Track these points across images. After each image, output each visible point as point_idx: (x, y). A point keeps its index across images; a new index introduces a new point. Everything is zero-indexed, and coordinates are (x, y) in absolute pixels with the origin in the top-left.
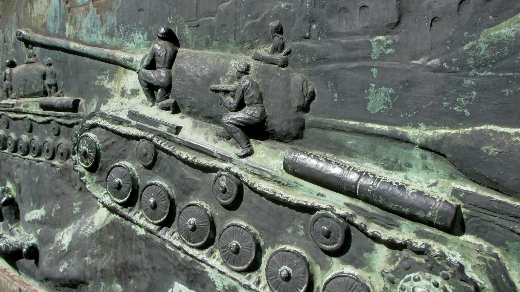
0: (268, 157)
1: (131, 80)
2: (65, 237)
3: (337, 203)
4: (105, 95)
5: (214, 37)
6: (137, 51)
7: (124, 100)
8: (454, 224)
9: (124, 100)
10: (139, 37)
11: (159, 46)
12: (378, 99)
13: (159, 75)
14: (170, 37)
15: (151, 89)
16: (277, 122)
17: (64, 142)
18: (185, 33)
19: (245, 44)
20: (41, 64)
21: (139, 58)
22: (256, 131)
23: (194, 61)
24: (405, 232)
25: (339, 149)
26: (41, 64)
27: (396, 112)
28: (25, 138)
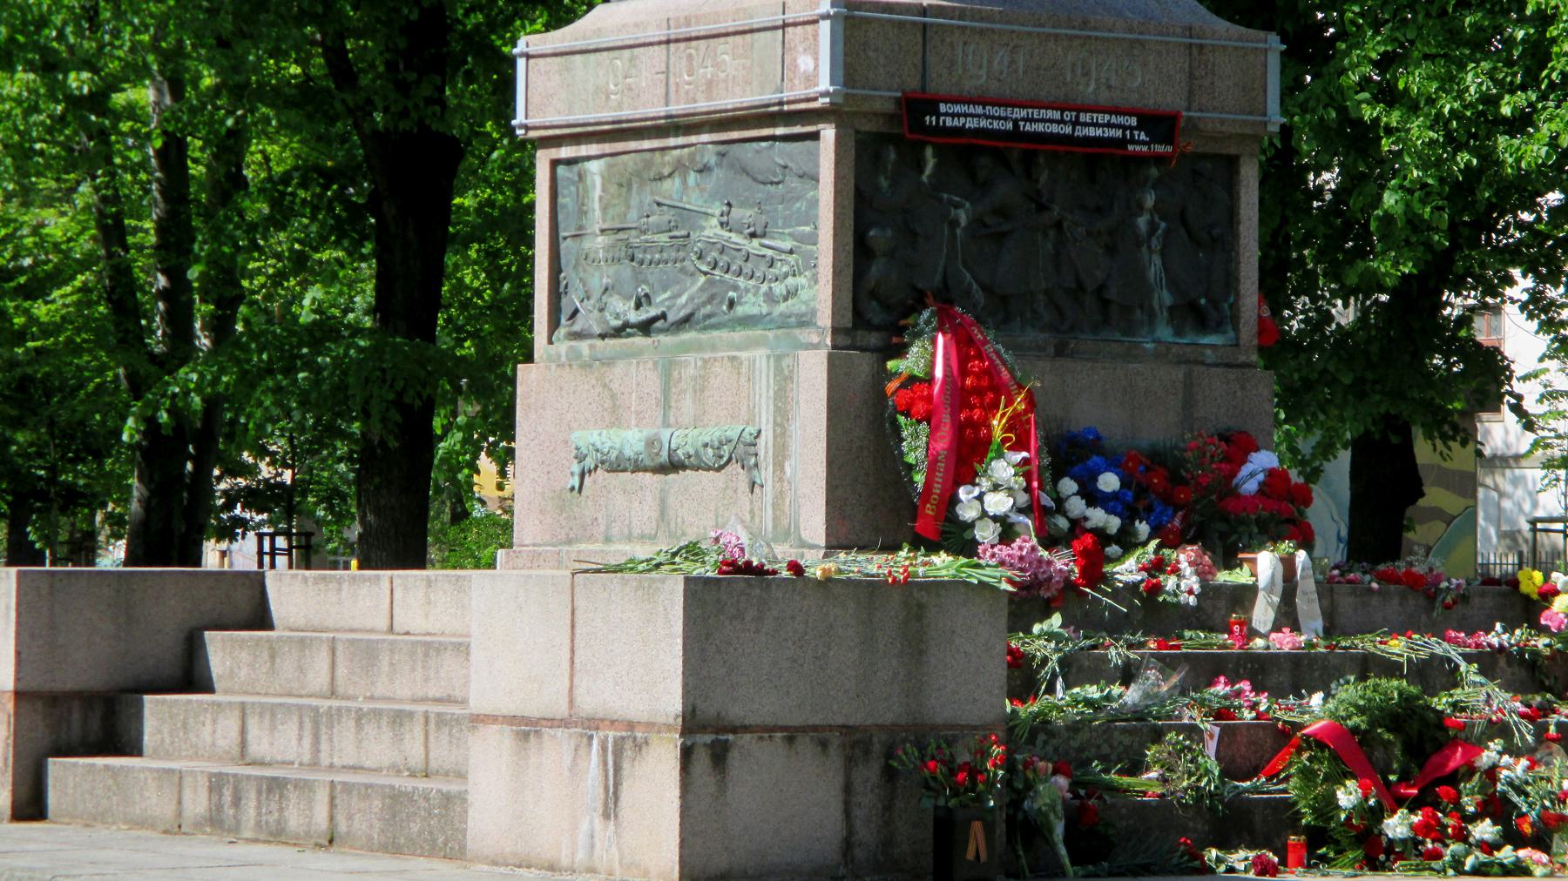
0: (756, 242)
1: (714, 221)
2: (683, 299)
3: (770, 253)
4: (703, 228)
5: (742, 205)
6: (717, 208)
7: (711, 229)
8: (791, 252)
9: (711, 229)
10: (718, 204)
11: (725, 208)
12: (780, 223)
13: (725, 219)
14: (729, 204)
15: (722, 224)
16: (759, 231)
17: (682, 254)
18: (733, 202)
19: (751, 207)
20: (669, 215)
21: (717, 212)
22: (753, 235)
23: (736, 212)
24: (783, 256)
25: (773, 238)
26: (669, 215)
27: (785, 226)
28: (657, 256)
